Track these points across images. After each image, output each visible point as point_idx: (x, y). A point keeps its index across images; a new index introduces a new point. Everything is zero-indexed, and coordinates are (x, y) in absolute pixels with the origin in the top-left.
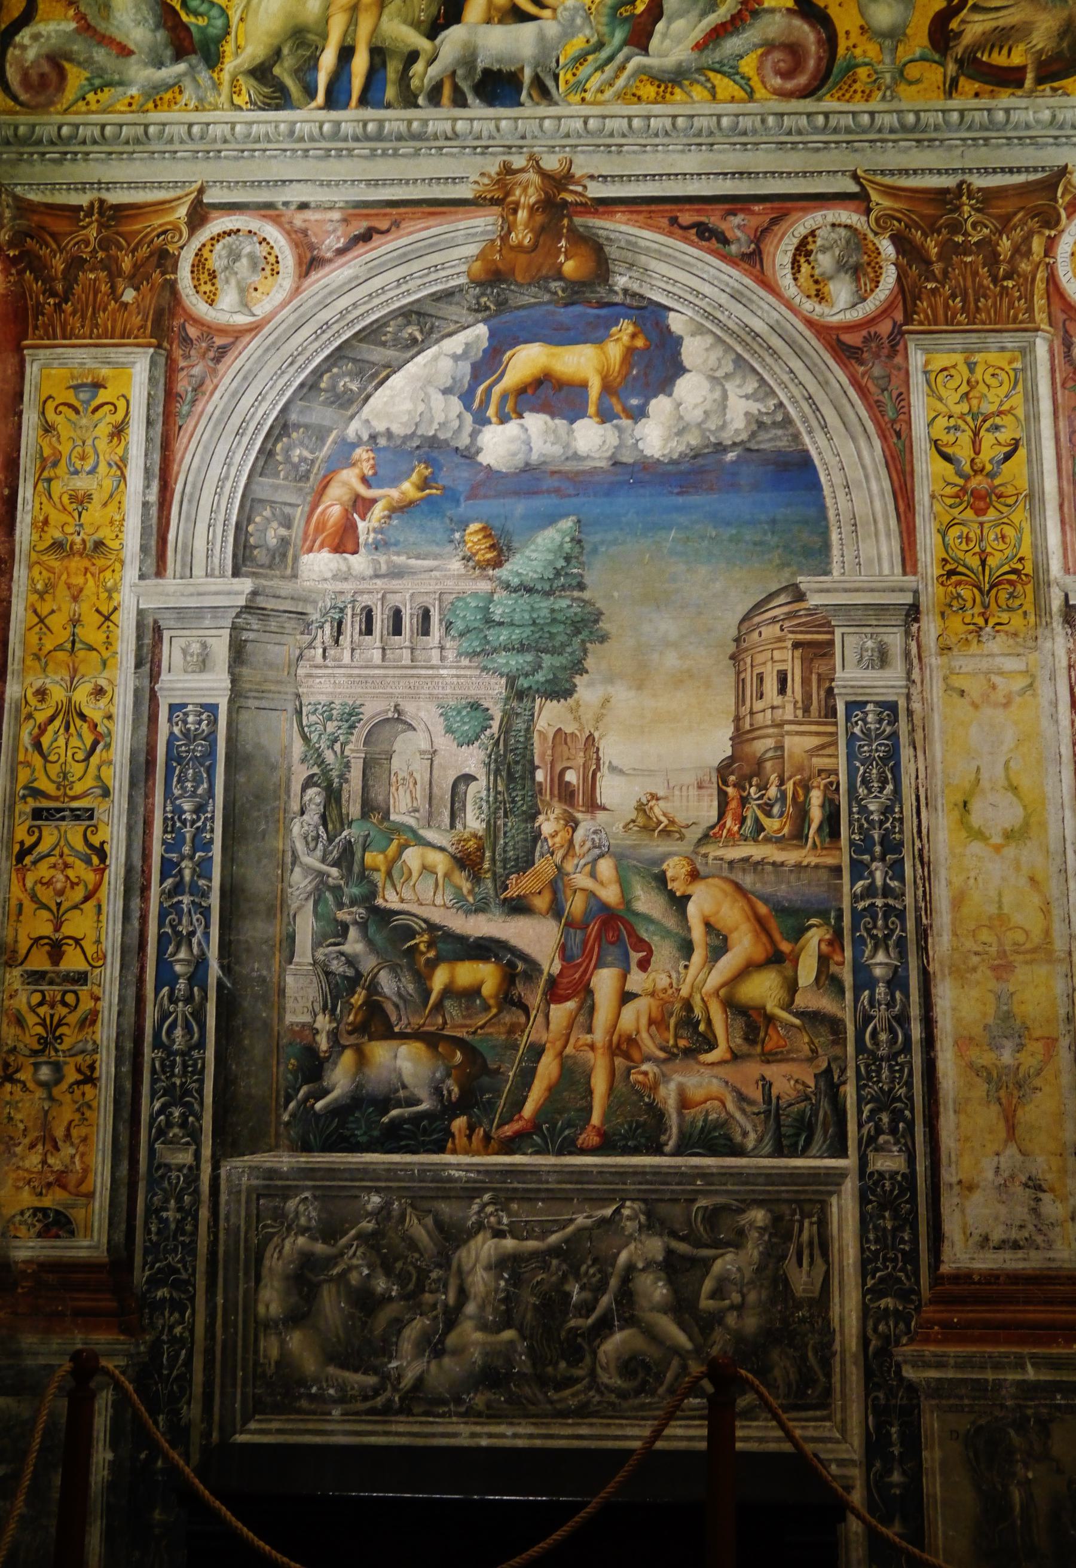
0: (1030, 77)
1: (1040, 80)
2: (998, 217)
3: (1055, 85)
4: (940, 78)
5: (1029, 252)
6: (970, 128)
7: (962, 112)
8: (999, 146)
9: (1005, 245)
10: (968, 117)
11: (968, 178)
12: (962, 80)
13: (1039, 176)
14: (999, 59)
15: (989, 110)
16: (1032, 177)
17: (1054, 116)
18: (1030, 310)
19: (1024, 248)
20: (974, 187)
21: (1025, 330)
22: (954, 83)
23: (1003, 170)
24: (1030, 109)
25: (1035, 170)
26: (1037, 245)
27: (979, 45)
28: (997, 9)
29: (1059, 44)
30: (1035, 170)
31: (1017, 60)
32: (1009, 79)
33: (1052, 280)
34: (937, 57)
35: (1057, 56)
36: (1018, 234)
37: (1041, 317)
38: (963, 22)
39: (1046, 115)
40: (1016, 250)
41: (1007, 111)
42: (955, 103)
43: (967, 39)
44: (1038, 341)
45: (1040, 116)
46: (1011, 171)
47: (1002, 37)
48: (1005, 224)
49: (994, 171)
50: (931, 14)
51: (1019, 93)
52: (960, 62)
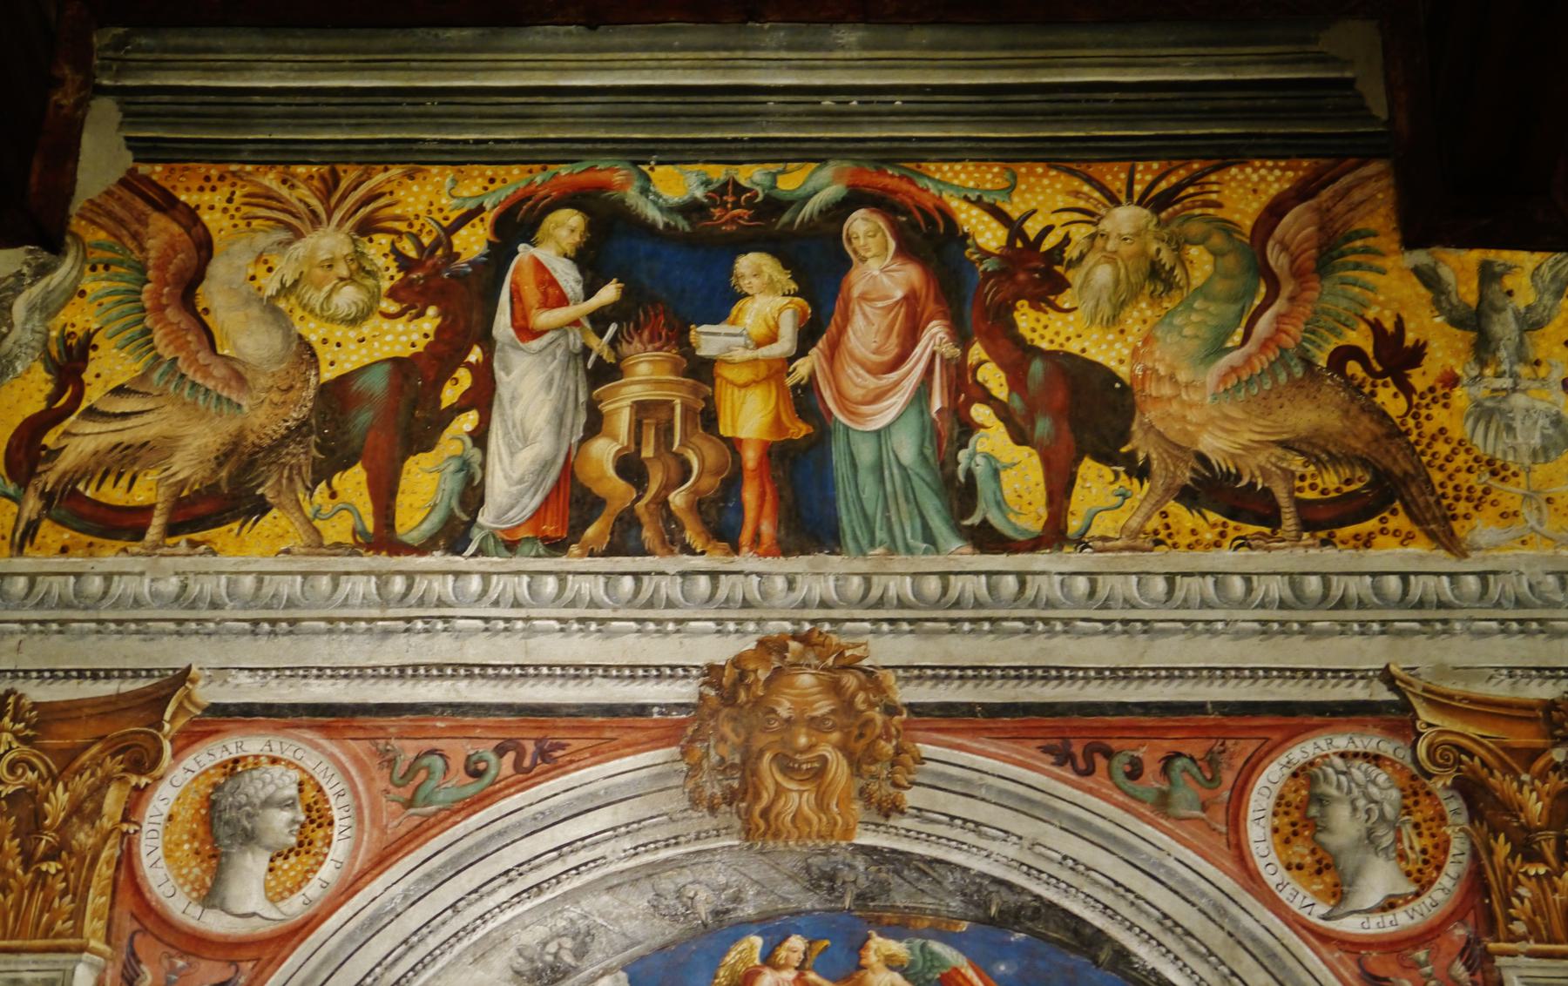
0: (158, 521)
1: (172, 530)
2: (55, 753)
3: (196, 536)
4: (9, 521)
5: (98, 812)
6: (39, 605)
7: (32, 578)
8: (83, 634)
9: (59, 800)
10: (42, 586)
11: (19, 686)
12: (46, 525)
13: (141, 684)
14: (113, 494)
15: (78, 575)
16: (128, 686)
17: (184, 587)
18: (78, 915)
19: (89, 806)
20: (26, 702)
21: (62, 950)
22: (31, 530)
23: (81, 674)
24: (142, 574)
25: (136, 674)
26: (113, 800)
27: (83, 473)
28: (125, 416)
29: (214, 472)
30: (136, 674)
31: (141, 495)
32: (124, 525)
33: (127, 861)
34: (11, 488)
35: (210, 491)
36: (82, 784)
37: (93, 927)
38: (66, 434)
39: (171, 585)
40: (76, 809)
41: (108, 577)
42: (24, 563)
43: (66, 462)
44: (81, 970)
45: (161, 586)
46: (95, 675)
47: (124, 460)
48: (67, 762)
49: (67, 674)
50: (18, 421)
51: (135, 547)
52: (47, 498)
